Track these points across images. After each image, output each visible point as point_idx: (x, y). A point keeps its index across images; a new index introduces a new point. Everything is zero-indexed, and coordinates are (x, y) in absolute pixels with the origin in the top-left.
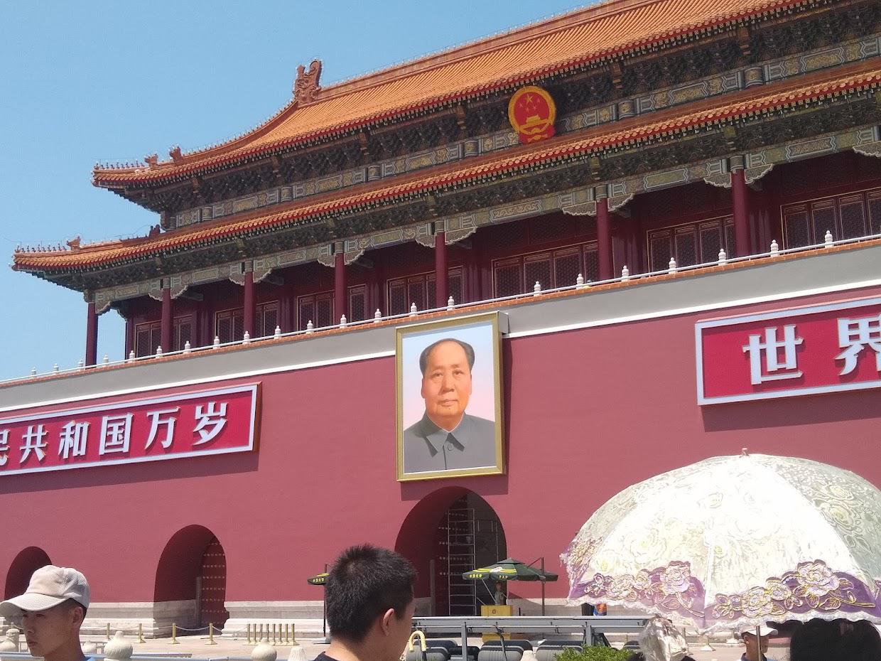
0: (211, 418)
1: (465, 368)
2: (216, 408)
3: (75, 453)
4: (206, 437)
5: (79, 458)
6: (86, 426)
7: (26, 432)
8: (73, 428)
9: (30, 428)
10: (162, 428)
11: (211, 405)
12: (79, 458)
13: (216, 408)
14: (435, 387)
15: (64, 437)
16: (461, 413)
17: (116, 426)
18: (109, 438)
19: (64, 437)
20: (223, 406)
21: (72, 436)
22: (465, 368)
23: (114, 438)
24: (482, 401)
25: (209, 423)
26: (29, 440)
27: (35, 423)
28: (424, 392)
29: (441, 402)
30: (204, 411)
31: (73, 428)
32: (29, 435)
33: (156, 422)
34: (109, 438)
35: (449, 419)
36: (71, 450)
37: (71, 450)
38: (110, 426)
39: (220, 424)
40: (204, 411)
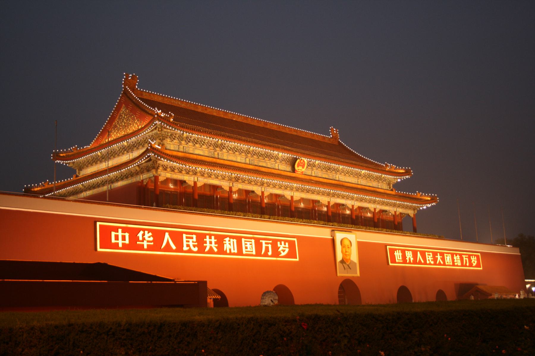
0: (284, 247)
1: (350, 246)
2: (285, 244)
3: (232, 251)
4: (283, 254)
5: (234, 254)
6: (235, 241)
8: (229, 241)
9: (208, 237)
10: (267, 248)
11: (283, 242)
12: (234, 254)
13: (285, 244)
14: (344, 251)
16: (350, 259)
17: (248, 243)
18: (246, 248)
20: (287, 244)
21: (230, 244)
22: (350, 246)
23: (248, 248)
24: (354, 257)
25: (283, 249)
26: (208, 242)
28: (342, 252)
29: (346, 255)
30: (281, 244)
31: (229, 241)
33: (264, 246)
34: (246, 248)
35: (347, 260)
36: (230, 250)
37: (230, 250)
38: (246, 243)
39: (287, 250)
40: (281, 244)
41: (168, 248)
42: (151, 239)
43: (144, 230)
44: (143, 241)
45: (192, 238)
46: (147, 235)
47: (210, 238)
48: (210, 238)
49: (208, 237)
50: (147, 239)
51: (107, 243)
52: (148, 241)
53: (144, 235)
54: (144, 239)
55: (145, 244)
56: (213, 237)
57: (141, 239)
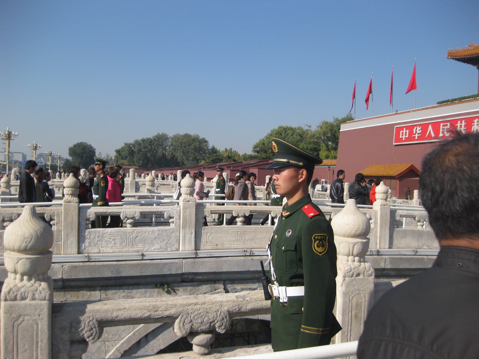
7: (457, 123)
9: (459, 122)
15: (474, 125)
19: (474, 125)
27: (461, 120)
32: (459, 125)
41: (430, 136)
42: (420, 131)
43: (417, 125)
44: (415, 134)
45: (447, 125)
46: (419, 128)
47: (461, 123)
48: (461, 123)
49: (459, 122)
50: (418, 132)
51: (398, 139)
52: (418, 134)
53: (416, 129)
54: (416, 132)
55: (417, 135)
56: (463, 121)
57: (414, 133)
